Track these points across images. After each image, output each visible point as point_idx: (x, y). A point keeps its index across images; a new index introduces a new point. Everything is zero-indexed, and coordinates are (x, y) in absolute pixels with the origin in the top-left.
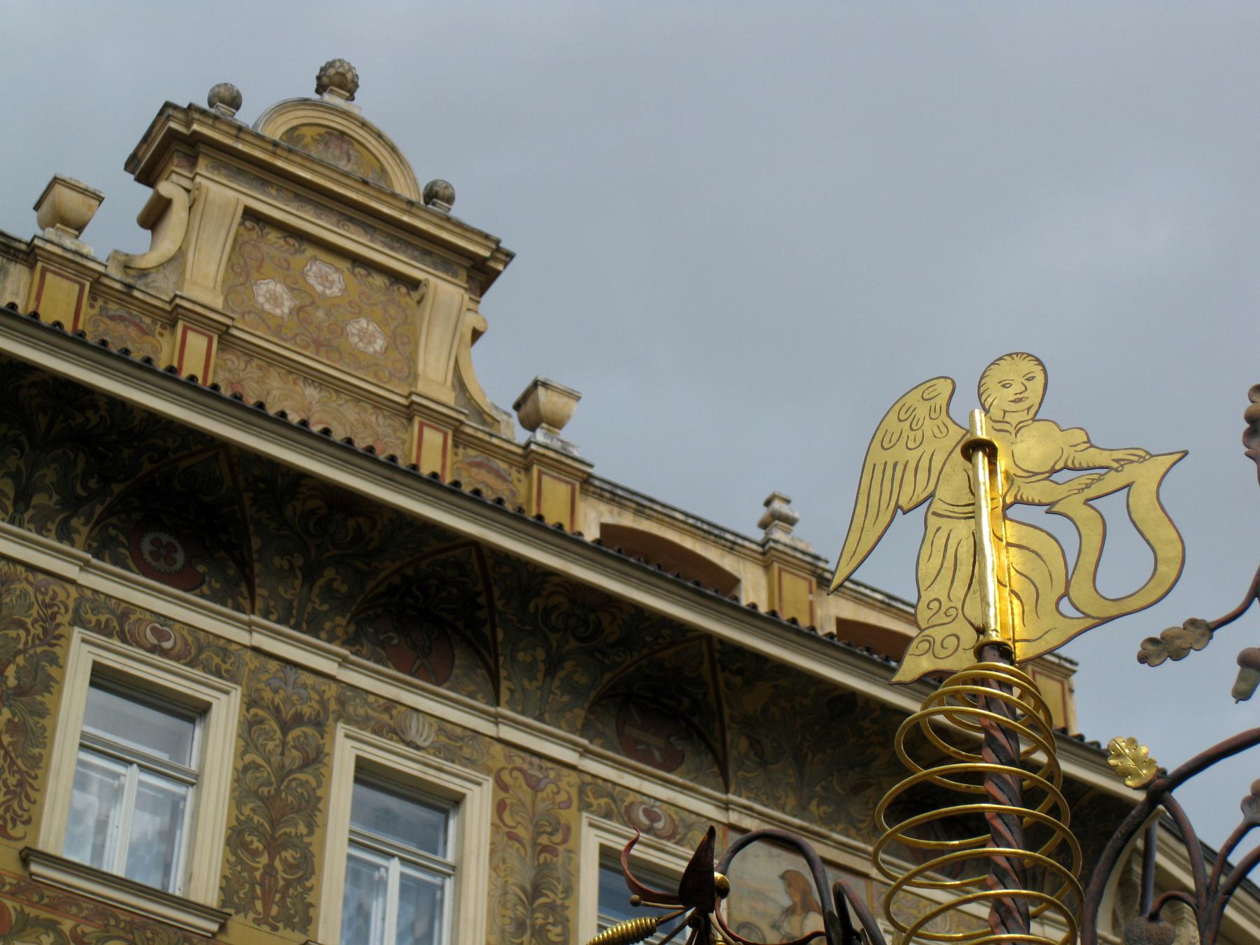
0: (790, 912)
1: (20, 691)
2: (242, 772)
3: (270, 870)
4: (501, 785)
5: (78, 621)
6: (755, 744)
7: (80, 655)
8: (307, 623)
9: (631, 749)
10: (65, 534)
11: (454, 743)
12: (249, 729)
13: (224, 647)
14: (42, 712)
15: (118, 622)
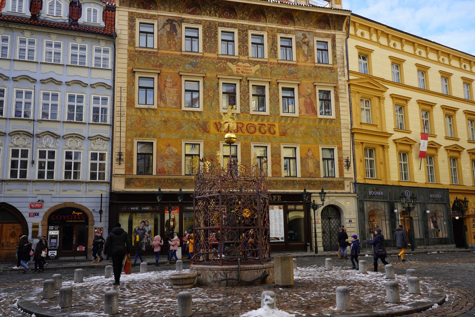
0: (303, 39)
1: (214, 36)
2: (239, 39)
3: (243, 50)
4: (268, 32)
5: (219, 26)
6: (298, 19)
7: (220, 29)
8: (243, 19)
9: (283, 24)
10: (216, 16)
11: (262, 29)
12: (239, 34)
13: (235, 24)
14: (217, 38)
15: (223, 25)
